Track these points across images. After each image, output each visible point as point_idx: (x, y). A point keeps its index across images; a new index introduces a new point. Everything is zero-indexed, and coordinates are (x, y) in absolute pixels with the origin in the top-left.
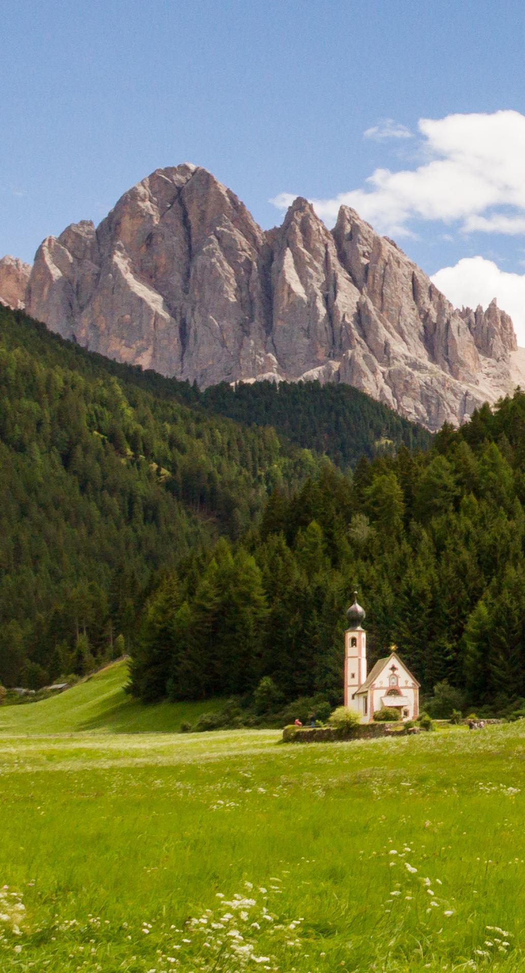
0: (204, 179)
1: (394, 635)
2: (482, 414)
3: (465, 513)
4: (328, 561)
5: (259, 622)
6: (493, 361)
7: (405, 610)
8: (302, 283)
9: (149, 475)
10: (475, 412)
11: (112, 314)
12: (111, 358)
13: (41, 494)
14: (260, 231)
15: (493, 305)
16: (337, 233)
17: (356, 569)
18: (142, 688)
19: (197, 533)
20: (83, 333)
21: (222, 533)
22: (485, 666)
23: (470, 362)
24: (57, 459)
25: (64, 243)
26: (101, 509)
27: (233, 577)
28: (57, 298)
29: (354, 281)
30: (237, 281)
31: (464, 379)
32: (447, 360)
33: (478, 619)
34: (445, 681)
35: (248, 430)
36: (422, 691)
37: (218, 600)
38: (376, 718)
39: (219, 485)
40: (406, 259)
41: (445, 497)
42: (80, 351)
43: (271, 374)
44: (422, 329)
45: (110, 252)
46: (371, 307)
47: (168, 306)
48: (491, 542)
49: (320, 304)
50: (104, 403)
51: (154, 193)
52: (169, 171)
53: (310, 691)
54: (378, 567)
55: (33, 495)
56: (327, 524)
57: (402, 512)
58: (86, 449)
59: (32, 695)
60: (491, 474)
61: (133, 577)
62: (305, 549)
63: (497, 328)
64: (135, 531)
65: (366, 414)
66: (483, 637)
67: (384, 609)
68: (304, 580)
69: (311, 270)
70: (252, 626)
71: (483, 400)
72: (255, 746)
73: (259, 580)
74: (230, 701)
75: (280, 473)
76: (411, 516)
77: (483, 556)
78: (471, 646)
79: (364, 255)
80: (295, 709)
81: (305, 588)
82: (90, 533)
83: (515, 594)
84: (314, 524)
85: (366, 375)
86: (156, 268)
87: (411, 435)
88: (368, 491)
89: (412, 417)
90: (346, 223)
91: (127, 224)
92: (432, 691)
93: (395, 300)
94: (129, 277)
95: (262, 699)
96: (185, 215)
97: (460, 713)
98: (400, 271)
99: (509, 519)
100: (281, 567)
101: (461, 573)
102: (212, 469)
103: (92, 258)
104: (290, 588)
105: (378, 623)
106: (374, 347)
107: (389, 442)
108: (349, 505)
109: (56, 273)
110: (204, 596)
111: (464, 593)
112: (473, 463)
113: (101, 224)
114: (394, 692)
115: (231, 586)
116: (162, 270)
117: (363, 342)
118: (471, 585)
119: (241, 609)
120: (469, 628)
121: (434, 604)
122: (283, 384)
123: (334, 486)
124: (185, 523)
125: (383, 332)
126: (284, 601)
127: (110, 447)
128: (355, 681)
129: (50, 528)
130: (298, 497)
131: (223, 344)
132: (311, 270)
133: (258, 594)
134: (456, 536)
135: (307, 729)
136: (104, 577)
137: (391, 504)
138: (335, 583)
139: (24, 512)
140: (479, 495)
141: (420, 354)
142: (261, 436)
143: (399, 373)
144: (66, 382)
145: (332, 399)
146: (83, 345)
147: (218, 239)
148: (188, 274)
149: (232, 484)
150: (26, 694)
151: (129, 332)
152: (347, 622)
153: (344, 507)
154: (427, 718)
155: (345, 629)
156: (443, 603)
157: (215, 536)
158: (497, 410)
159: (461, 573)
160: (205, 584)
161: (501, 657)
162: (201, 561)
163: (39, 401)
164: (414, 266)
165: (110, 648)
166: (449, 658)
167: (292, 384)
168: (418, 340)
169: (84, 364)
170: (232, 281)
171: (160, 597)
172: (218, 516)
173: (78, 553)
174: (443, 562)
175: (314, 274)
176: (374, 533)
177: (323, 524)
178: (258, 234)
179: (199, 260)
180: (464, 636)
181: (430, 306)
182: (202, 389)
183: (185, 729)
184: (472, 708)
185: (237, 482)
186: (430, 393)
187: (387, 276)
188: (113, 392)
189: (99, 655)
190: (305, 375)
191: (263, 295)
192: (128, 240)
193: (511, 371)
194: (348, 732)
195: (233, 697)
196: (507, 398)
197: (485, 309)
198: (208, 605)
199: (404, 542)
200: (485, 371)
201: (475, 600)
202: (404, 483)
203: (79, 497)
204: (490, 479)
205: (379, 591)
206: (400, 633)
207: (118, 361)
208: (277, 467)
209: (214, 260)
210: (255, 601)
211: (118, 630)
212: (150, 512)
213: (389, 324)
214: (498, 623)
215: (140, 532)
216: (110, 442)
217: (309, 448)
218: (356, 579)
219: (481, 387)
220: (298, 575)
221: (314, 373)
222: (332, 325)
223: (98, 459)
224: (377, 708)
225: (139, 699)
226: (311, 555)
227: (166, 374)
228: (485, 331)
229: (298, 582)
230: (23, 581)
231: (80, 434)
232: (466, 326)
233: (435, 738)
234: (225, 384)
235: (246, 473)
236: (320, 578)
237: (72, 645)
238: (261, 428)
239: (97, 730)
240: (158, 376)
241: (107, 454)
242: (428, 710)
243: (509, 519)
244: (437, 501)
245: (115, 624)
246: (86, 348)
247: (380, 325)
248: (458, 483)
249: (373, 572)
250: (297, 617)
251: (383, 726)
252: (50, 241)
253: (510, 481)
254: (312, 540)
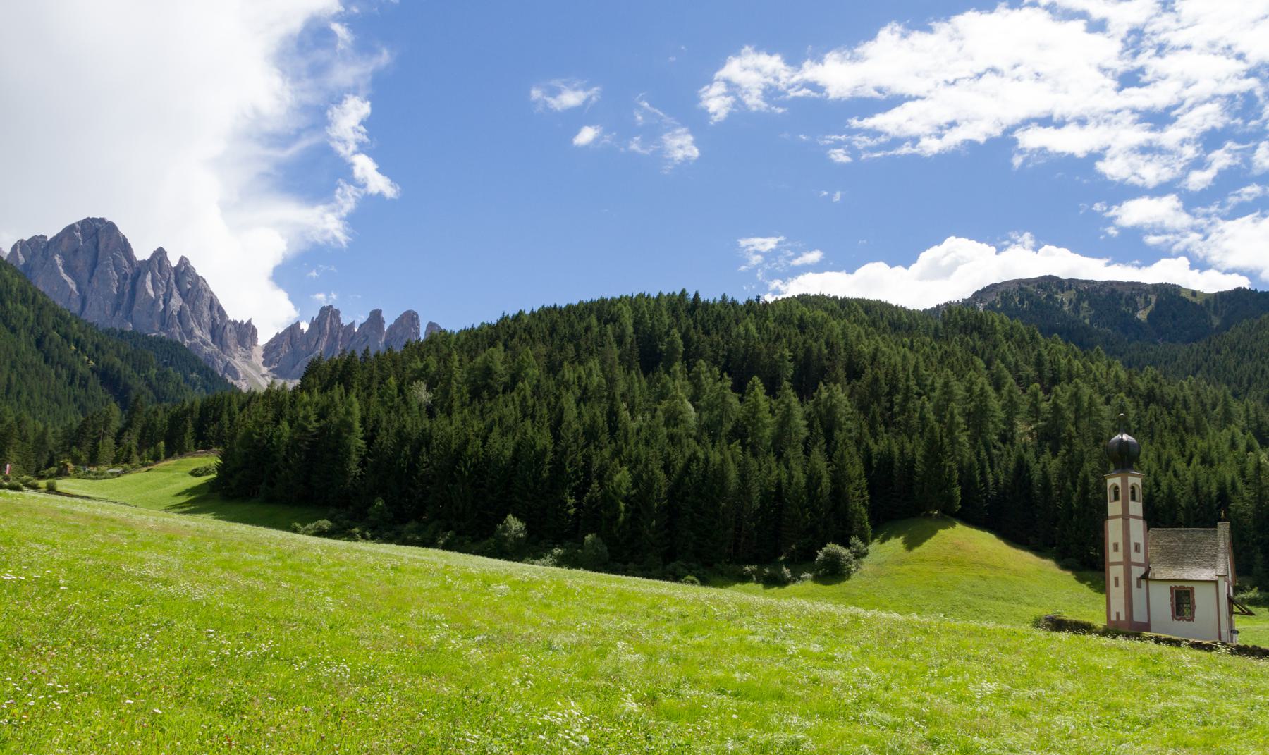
15: (250, 321)
16: (176, 269)
23: (232, 347)
29: (181, 295)
46: (188, 309)
91: (66, 241)
98: (206, 295)
141: (209, 339)
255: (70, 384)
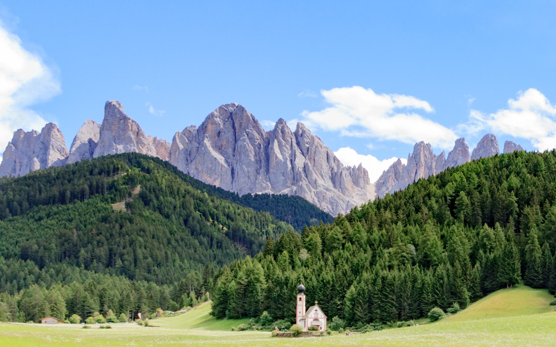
0: (241, 109)
1: (317, 297)
2: (354, 211)
3: (347, 250)
4: (291, 267)
5: (262, 290)
6: (360, 189)
7: (322, 288)
8: (281, 154)
9: (219, 229)
10: (352, 210)
11: (204, 164)
12: (203, 182)
13: (176, 235)
14: (264, 131)
15: (360, 165)
16: (296, 134)
17: (301, 271)
18: (216, 313)
19: (238, 254)
20: (192, 171)
21: (248, 254)
22: (353, 311)
23: (350, 189)
24: (182, 221)
25: (184, 134)
26: (199, 242)
27: (252, 271)
28: (182, 157)
29: (303, 154)
30: (255, 152)
31: (347, 196)
32: (341, 188)
33: (351, 293)
34: (337, 317)
35: (259, 213)
36: (328, 320)
37: (246, 280)
38: (309, 330)
39: (247, 235)
40: (325, 145)
41: (338, 243)
42: (192, 178)
43: (268, 191)
44: (331, 175)
45: (203, 138)
46: (309, 165)
47: (227, 161)
48: (357, 262)
49: (289, 163)
50: (201, 200)
51: (221, 115)
52: (227, 106)
53: (282, 318)
54: (310, 270)
55: (172, 235)
56: (291, 252)
57: (321, 248)
58: (193, 218)
59: (173, 314)
60: (358, 235)
61: (212, 269)
62: (281, 262)
63: (362, 175)
64: (213, 252)
65: (307, 208)
66: (352, 300)
67: (313, 287)
68: (281, 274)
69: (285, 149)
70: (260, 291)
71: (355, 205)
72: (261, 338)
73: (263, 273)
74: (251, 320)
75: (271, 231)
76: (324, 250)
77: (354, 268)
78: (348, 303)
79: (307, 143)
80: (277, 324)
81: (281, 277)
82: (195, 252)
83: (366, 283)
84: (285, 252)
85: (307, 193)
86: (222, 146)
87: (325, 218)
88: (307, 239)
89: (326, 211)
90: (300, 129)
91: (210, 127)
92: (332, 320)
93: (320, 162)
94: (211, 149)
95: (264, 319)
96: (234, 124)
97: (343, 329)
98: (322, 150)
99: (365, 253)
100: (271, 268)
101: (345, 274)
102: (244, 228)
103: (195, 141)
104: (275, 277)
105: (310, 292)
106: (310, 181)
107: (316, 220)
108: (299, 245)
109: (181, 146)
110: (240, 278)
111: (345, 282)
112: (351, 231)
113: (199, 127)
114: (316, 320)
115: (252, 275)
116: (224, 146)
117: (306, 179)
118: (349, 279)
119: (255, 284)
120: (347, 296)
121: (333, 286)
122: (273, 195)
123: (293, 237)
124: (233, 249)
125: (314, 175)
126: (273, 282)
127: (203, 218)
128: (301, 315)
129: (179, 249)
130: (279, 241)
131: (249, 178)
132: (285, 149)
133: (262, 279)
134: (343, 259)
135: (281, 332)
136: (201, 269)
137: (316, 245)
138: (293, 276)
139: (169, 242)
140: (353, 243)
141: (330, 184)
142: (264, 216)
143: (321, 192)
144: (185, 191)
145: (293, 202)
146: (192, 176)
147: (247, 134)
148: (235, 149)
149: (253, 234)
150: (171, 313)
151: (211, 171)
152: (298, 291)
153: (298, 246)
154: (329, 330)
155: (297, 294)
156: (337, 286)
157: (245, 255)
158: (361, 209)
159: (345, 274)
160: (241, 274)
161: (360, 308)
162: (240, 264)
163: (174, 198)
164: (327, 148)
165: (203, 297)
166: (339, 307)
167: (277, 195)
168: (329, 179)
169: (193, 184)
170: (253, 152)
171: (222, 279)
172: (247, 247)
173: (191, 259)
174: (337, 269)
175: (286, 150)
176: (310, 256)
177: (289, 252)
178: (263, 133)
179: (239, 143)
180: (345, 299)
181: (334, 165)
182: (240, 196)
183: (233, 330)
184: (348, 328)
185: (254, 234)
186: (333, 201)
187: (316, 152)
188: (204, 196)
189: (199, 300)
190: (282, 191)
191: (265, 158)
192: (210, 134)
193: (367, 194)
194: (298, 335)
195: (252, 318)
196: (365, 204)
197: (357, 167)
198: (242, 282)
199: (322, 260)
200: (356, 192)
201: (350, 284)
202: (322, 237)
203: (191, 237)
204: (357, 237)
205: (311, 280)
206: (319, 297)
207: (206, 183)
208: (271, 227)
209: (245, 143)
210: (261, 282)
211: (207, 290)
212: (219, 244)
213: (317, 172)
214: (359, 294)
215: (215, 252)
216: (203, 216)
217: (284, 221)
218: (302, 275)
219: (354, 199)
220: (278, 272)
221: (286, 191)
222: (293, 171)
223: (198, 222)
224: (309, 325)
225: (215, 317)
226: (284, 264)
227: (226, 189)
228: (357, 175)
229: (278, 274)
230: (169, 270)
231: (191, 212)
232: (349, 174)
233: (332, 339)
234: (250, 194)
235: (258, 231)
236: (287, 273)
237: (188, 294)
238: (264, 212)
239: (199, 329)
240: (222, 190)
241: (202, 220)
242: (330, 327)
243: (365, 253)
244: (335, 245)
245: (205, 288)
246: (193, 178)
247: (313, 172)
248: (344, 238)
249: (308, 272)
250: (278, 288)
251: (312, 333)
252: (178, 133)
253: (365, 238)
254: (284, 258)
255: (211, 247)
